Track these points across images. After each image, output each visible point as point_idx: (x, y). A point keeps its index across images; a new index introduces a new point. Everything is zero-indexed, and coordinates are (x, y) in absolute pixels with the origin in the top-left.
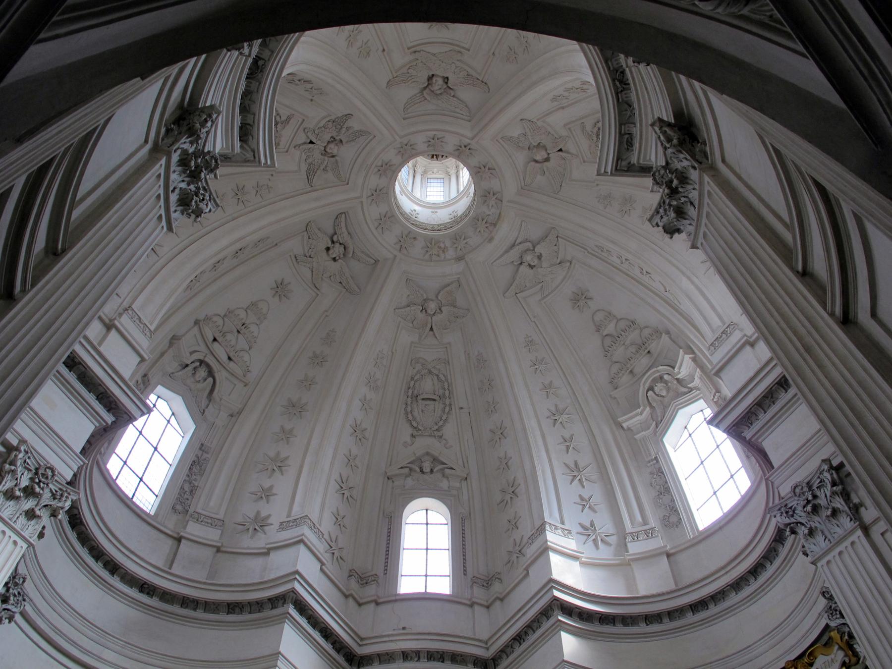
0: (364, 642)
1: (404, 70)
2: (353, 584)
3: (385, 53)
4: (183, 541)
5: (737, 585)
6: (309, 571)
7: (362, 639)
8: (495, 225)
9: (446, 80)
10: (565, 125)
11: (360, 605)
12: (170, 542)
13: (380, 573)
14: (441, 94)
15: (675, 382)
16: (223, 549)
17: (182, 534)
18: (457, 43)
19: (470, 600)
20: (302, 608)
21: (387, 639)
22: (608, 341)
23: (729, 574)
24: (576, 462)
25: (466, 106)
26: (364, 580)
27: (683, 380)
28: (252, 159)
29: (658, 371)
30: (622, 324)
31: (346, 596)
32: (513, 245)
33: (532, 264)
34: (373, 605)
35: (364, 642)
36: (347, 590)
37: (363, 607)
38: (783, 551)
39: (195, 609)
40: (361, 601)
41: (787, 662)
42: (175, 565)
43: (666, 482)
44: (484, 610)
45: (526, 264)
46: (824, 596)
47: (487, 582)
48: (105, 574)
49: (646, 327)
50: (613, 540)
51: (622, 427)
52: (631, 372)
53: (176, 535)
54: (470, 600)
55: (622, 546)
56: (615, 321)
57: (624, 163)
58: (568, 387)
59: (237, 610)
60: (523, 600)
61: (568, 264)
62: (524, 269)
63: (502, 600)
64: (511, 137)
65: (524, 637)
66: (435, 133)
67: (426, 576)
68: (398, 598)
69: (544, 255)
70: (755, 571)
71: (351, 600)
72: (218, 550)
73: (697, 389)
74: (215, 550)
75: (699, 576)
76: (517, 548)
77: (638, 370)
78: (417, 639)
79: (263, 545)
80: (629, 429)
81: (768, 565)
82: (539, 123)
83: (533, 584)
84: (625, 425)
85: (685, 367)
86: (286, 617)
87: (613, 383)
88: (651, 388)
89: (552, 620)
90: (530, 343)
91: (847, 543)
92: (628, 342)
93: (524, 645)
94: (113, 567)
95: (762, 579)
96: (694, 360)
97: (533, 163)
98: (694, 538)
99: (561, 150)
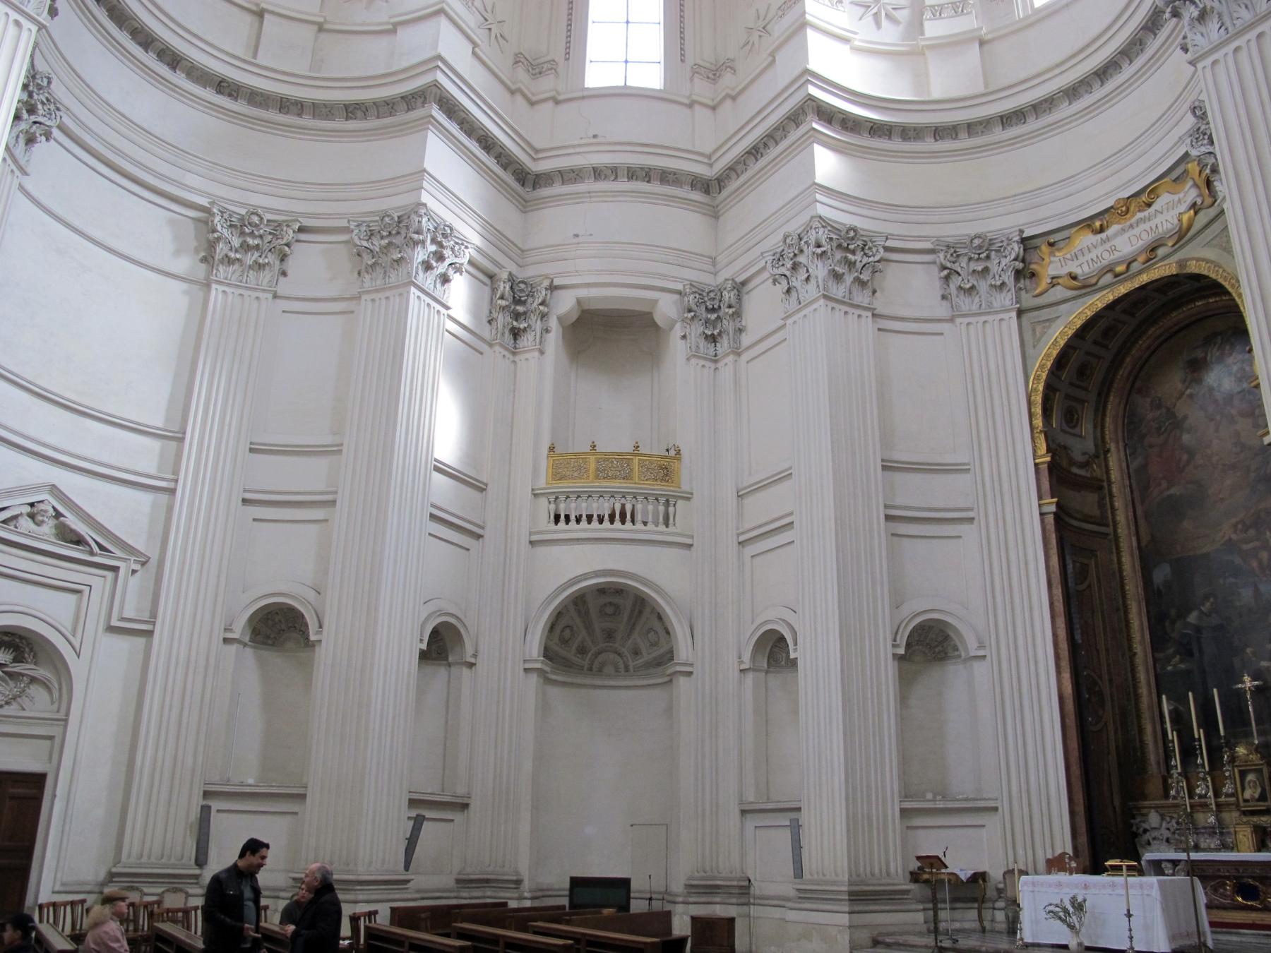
0: (541, 155)
2: (522, 74)
4: (267, 16)
6: (454, 54)
7: (537, 151)
11: (532, 104)
12: (248, 18)
13: (560, 58)
16: (327, 26)
17: (263, 5)
19: (688, 98)
20: (451, 108)
21: (571, 151)
23: (1065, 75)
26: (537, 68)
31: (512, 92)
34: (550, 104)
35: (541, 155)
36: (514, 83)
37: (536, 107)
38: (1153, 45)
39: (299, 115)
40: (534, 99)
41: (1118, 201)
42: (260, 53)
44: (708, 112)
46: (1194, 113)
47: (714, 73)
48: (164, 70)
50: (903, 15)
53: (254, 8)
54: (688, 98)
55: (916, 25)
59: (359, 114)
60: (762, 102)
63: (734, 98)
65: (762, 150)
67: (626, 62)
68: (585, 93)
70: (1102, 74)
71: (519, 98)
72: (321, 28)
74: (316, 28)
75: (1023, 75)
76: (761, 23)
79: (385, 19)
81: (1125, 65)
83: (783, 74)
86: (429, 122)
89: (803, 129)
93: (762, 162)
94: (173, 60)
95: (1111, 85)
98: (1024, 18)
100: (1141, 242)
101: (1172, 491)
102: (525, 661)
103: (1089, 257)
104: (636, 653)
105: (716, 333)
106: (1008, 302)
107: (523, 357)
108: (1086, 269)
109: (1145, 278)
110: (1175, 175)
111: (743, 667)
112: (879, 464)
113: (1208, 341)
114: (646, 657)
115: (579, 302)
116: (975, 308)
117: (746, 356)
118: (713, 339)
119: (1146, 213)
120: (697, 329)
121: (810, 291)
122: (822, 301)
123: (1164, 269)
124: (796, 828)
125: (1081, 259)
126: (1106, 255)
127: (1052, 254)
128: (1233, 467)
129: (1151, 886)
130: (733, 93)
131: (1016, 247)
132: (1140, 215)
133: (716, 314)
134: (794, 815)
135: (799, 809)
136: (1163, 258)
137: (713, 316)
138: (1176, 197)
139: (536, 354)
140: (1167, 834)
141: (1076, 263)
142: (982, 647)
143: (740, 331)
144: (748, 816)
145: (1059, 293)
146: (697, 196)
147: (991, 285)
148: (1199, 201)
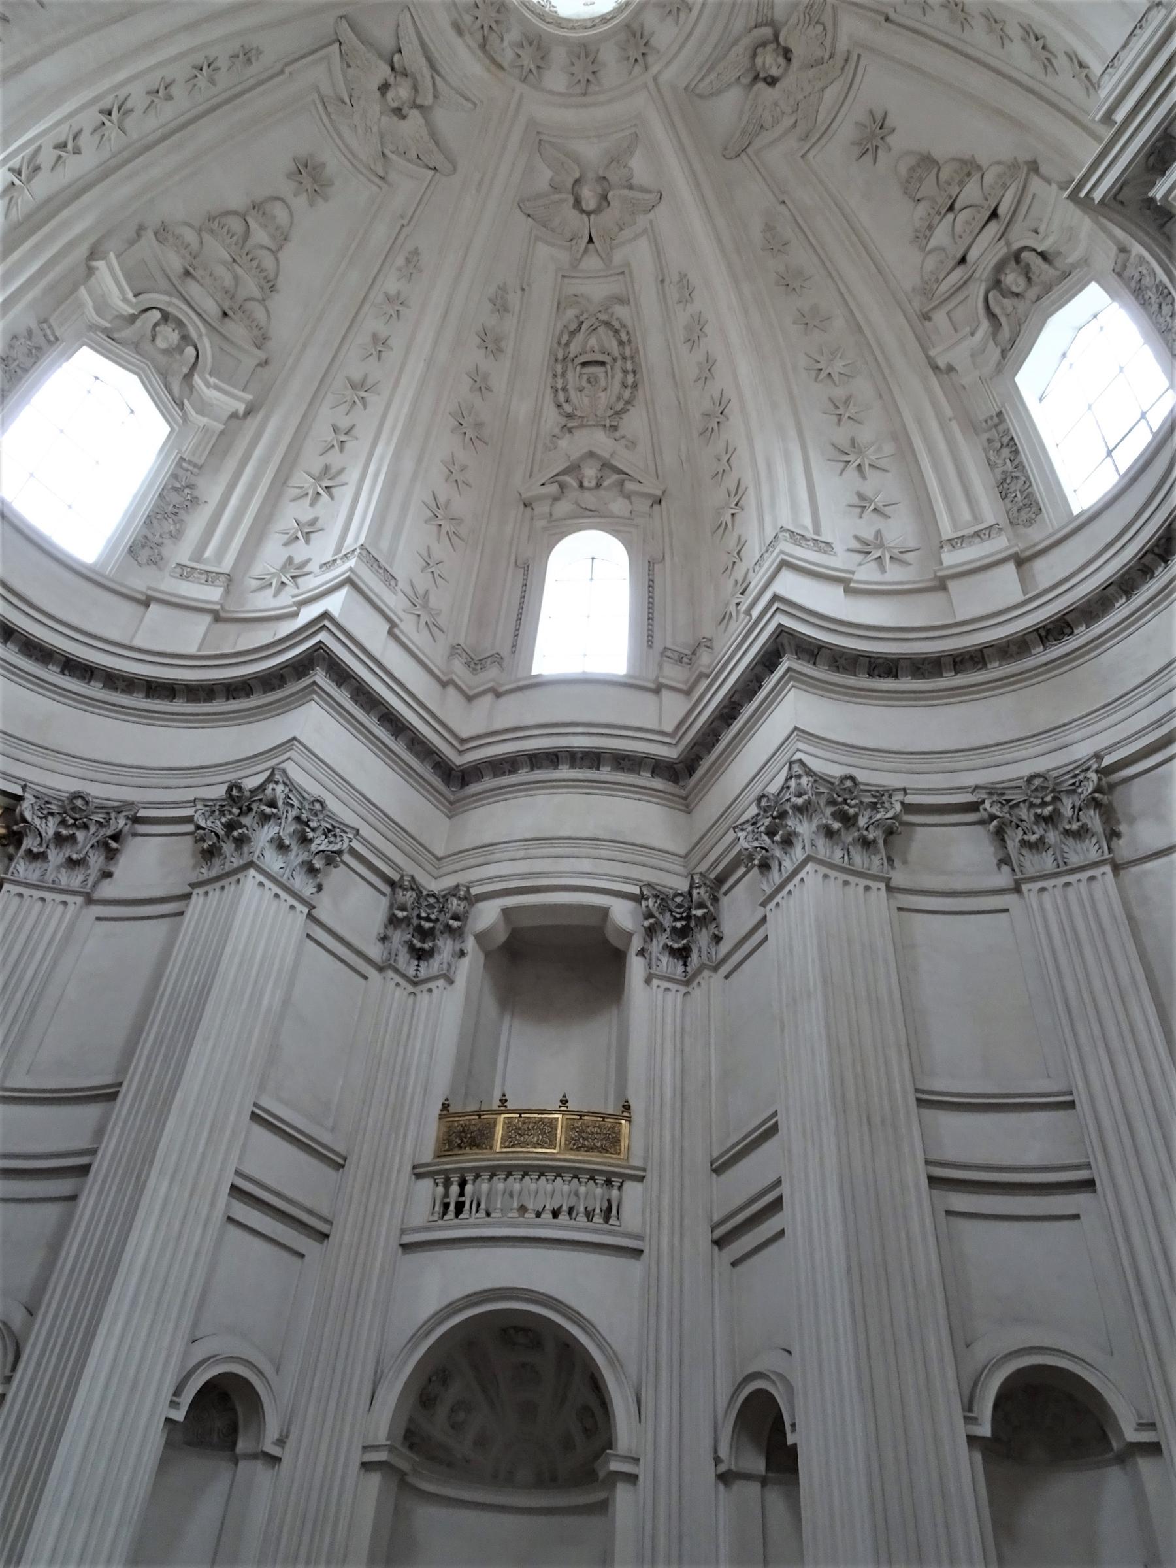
1: (827, 18)
3: (882, 19)
8: (483, 46)
9: (772, 81)
10: (629, 265)
14: (754, 55)
15: (185, 370)
18: (823, 141)
22: (236, 225)
24: (37, 169)
25: (712, 95)
27: (191, 387)
28: (1120, 197)
29: (200, 336)
30: (268, 262)
32: (433, 67)
33: (390, 95)
45: (391, 80)
49: (269, 316)
51: (93, 254)
52: (187, 273)
56: (273, 248)
57: (785, 642)
58: (158, 134)
61: (381, 173)
62: (384, 71)
64: (632, 154)
66: (695, 12)
69: (402, 122)
73: (185, 418)
77: (193, 289)
80: (90, 271)
82: (642, 221)
84: (100, 264)
85: (220, 398)
87: (163, 233)
88: (166, 317)
90: (247, 55)
92: (240, 271)
96: (234, 415)
97: (577, 175)
99: (591, 240)
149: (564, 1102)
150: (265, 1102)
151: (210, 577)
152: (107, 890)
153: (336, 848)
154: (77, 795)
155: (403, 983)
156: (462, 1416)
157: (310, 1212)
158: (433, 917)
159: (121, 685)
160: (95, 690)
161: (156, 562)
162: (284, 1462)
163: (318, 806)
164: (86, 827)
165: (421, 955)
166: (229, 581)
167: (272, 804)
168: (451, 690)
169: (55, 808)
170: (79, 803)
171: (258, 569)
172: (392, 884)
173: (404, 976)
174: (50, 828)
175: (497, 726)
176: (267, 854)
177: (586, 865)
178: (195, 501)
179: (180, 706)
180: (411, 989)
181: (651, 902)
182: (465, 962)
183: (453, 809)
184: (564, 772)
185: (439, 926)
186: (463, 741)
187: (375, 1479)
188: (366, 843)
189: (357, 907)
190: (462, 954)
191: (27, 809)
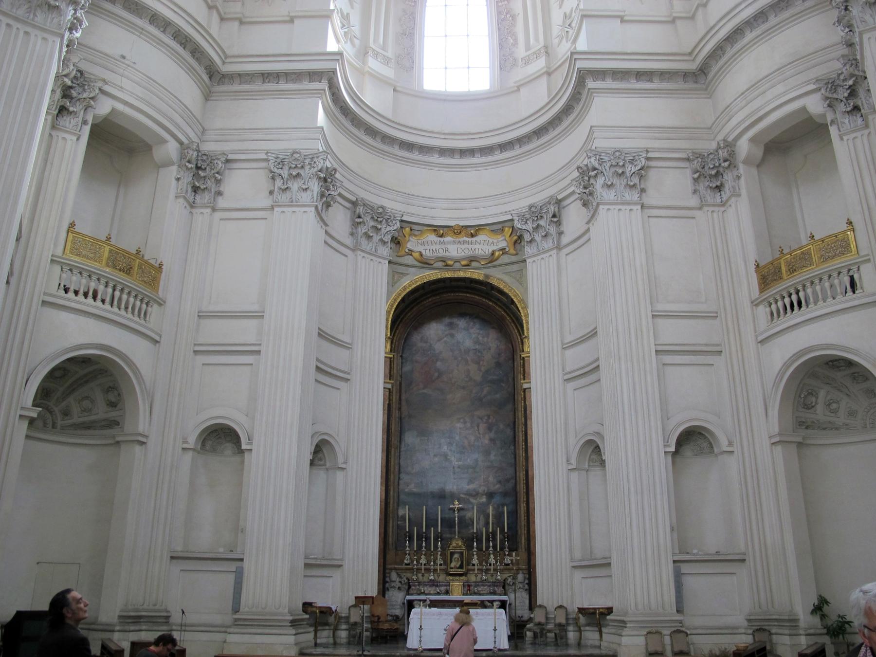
5: (443, 152)
43: (413, 29)
50: (357, 42)
70: (464, 152)
78: (175, 12)
91: (629, 207)
100: (463, 254)
101: (425, 391)
102: (22, 408)
103: (432, 247)
104: (66, 413)
105: (202, 187)
106: (385, 253)
107: (62, 135)
108: (428, 253)
109: (461, 274)
110: (497, 228)
111: (185, 446)
112: (317, 330)
113: (462, 315)
114: (76, 419)
115: (114, 110)
116: (368, 249)
117: (218, 215)
118: (196, 190)
119: (470, 239)
120: (187, 178)
121: (306, 197)
122: (313, 209)
123: (477, 274)
124: (239, 576)
125: (426, 247)
126: (441, 251)
127: (410, 235)
128: (464, 388)
129: (501, 614)
130: (244, 20)
131: (398, 223)
132: (467, 239)
133: (203, 174)
134: (239, 564)
135: (242, 560)
136: (474, 269)
137: (202, 173)
138: (491, 241)
139: (75, 138)
140: (399, 585)
141: (423, 247)
142: (345, 463)
143: (219, 193)
144: (175, 561)
145: (409, 260)
146: (206, 78)
147: (381, 240)
148: (507, 249)
149: (812, 237)
150: (660, 307)
151: (537, 55)
152: (565, 240)
153: (639, 167)
154: (531, 207)
155: (716, 209)
156: (834, 406)
157: (706, 345)
158: (717, 165)
159: (526, 140)
160: (517, 151)
161: (515, 64)
162: (736, 453)
163: (617, 154)
164: (542, 217)
165: (719, 188)
166: (547, 50)
167: (595, 169)
168: (679, 23)
169: (528, 216)
170: (533, 209)
171: (556, 30)
172: (688, 159)
173: (714, 205)
174: (530, 226)
175: (712, 24)
176: (604, 194)
177: (780, 88)
178: (514, 17)
179: (552, 134)
180: (722, 209)
181: (823, 91)
182: (742, 181)
183: (708, 91)
184: (749, 36)
185: (721, 170)
186: (690, 54)
187: (779, 449)
188: (660, 150)
189: (672, 184)
190: (738, 177)
191: (517, 225)
